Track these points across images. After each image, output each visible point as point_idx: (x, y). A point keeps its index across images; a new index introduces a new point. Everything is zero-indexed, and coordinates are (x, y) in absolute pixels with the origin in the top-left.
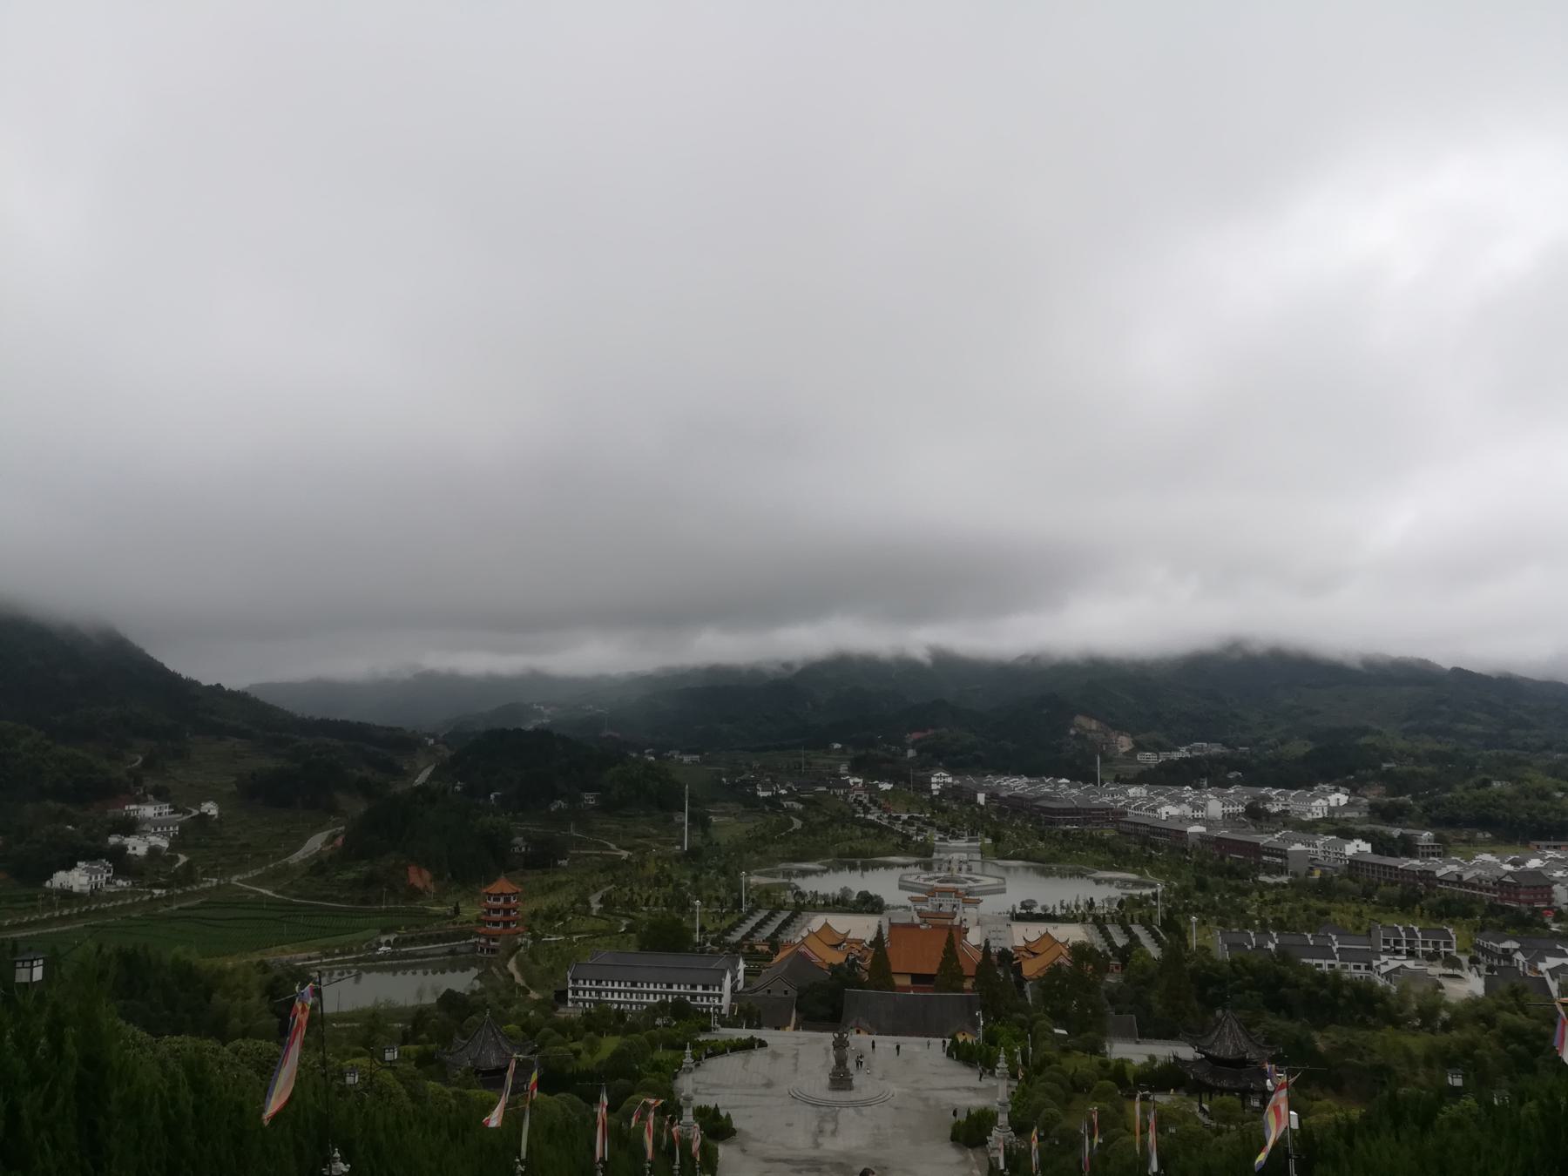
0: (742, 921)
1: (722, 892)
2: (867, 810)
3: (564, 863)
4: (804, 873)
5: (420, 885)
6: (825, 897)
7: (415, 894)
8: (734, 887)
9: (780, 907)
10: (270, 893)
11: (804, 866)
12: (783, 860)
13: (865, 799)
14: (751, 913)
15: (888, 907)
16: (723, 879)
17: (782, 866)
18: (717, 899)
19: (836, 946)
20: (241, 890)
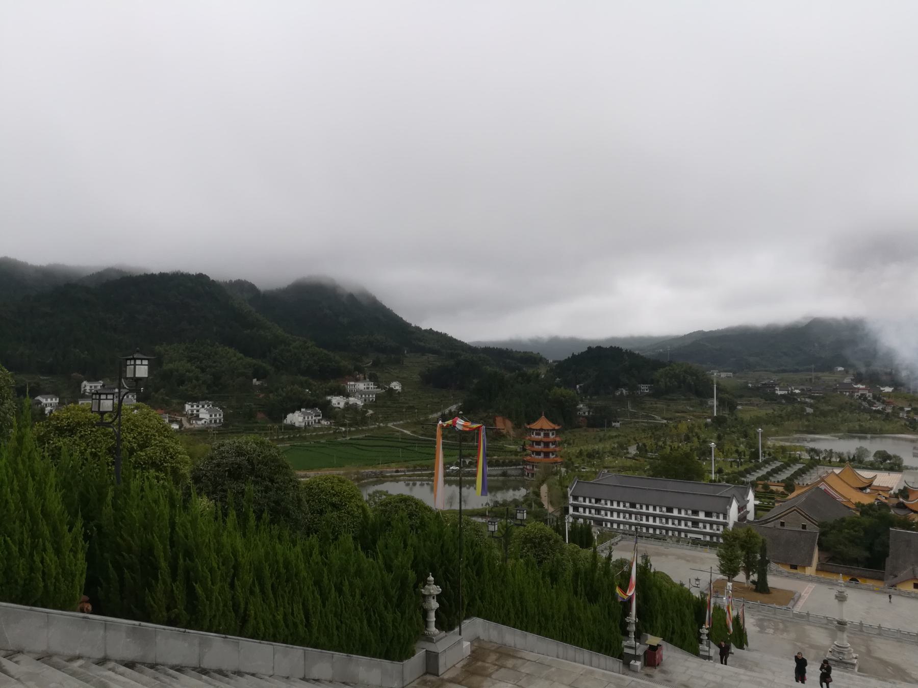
0: (758, 467)
1: (742, 447)
2: (871, 404)
3: (618, 425)
4: (813, 440)
6: (840, 455)
8: (752, 445)
9: (796, 460)
10: (408, 433)
11: (817, 436)
12: (798, 432)
13: (869, 395)
14: (766, 462)
15: (907, 468)
16: (742, 440)
17: (798, 436)
18: (737, 451)
19: (862, 489)
20: (393, 430)
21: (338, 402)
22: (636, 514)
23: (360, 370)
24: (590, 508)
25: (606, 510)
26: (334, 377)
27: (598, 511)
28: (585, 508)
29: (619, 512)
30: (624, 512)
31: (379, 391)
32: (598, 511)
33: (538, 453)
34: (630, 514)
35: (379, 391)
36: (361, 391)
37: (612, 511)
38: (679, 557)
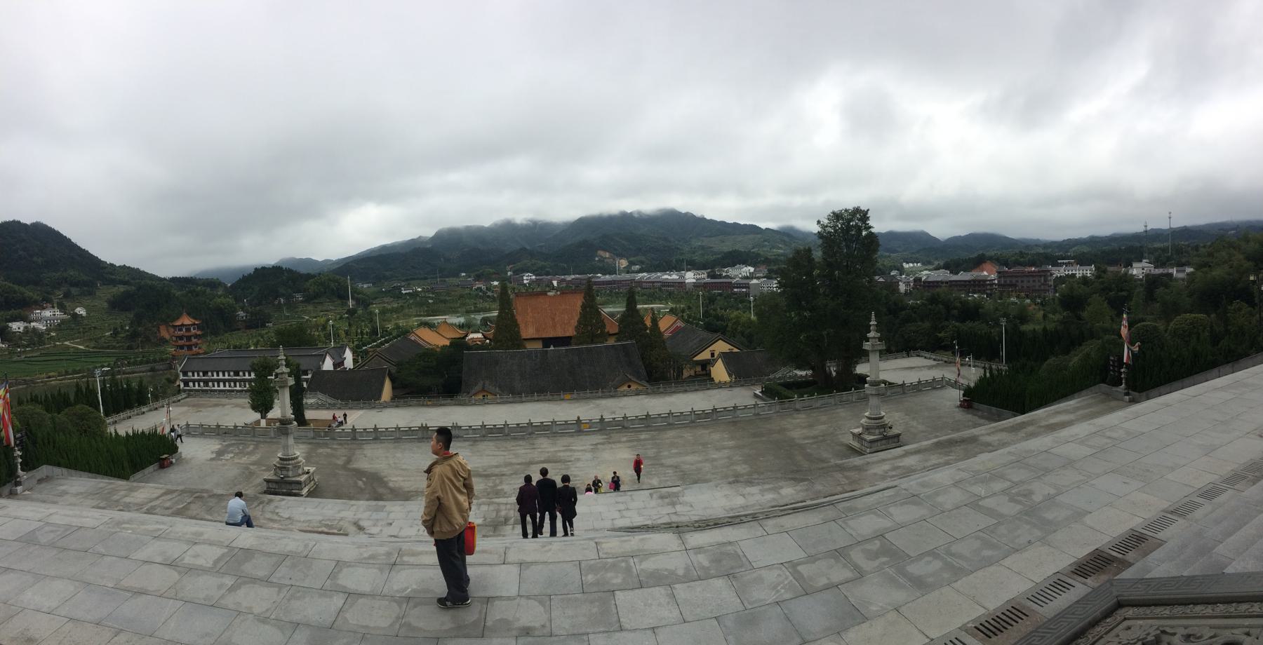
5: (167, 337)
7: (164, 341)
21: (17, 326)
22: (240, 381)
23: (49, 301)
24: (199, 381)
25: (213, 381)
26: (21, 308)
27: (206, 383)
28: (194, 381)
29: (224, 381)
30: (230, 381)
31: (65, 317)
32: (206, 383)
33: (182, 347)
34: (235, 382)
35: (65, 317)
36: (47, 316)
37: (218, 381)
38: (237, 406)
